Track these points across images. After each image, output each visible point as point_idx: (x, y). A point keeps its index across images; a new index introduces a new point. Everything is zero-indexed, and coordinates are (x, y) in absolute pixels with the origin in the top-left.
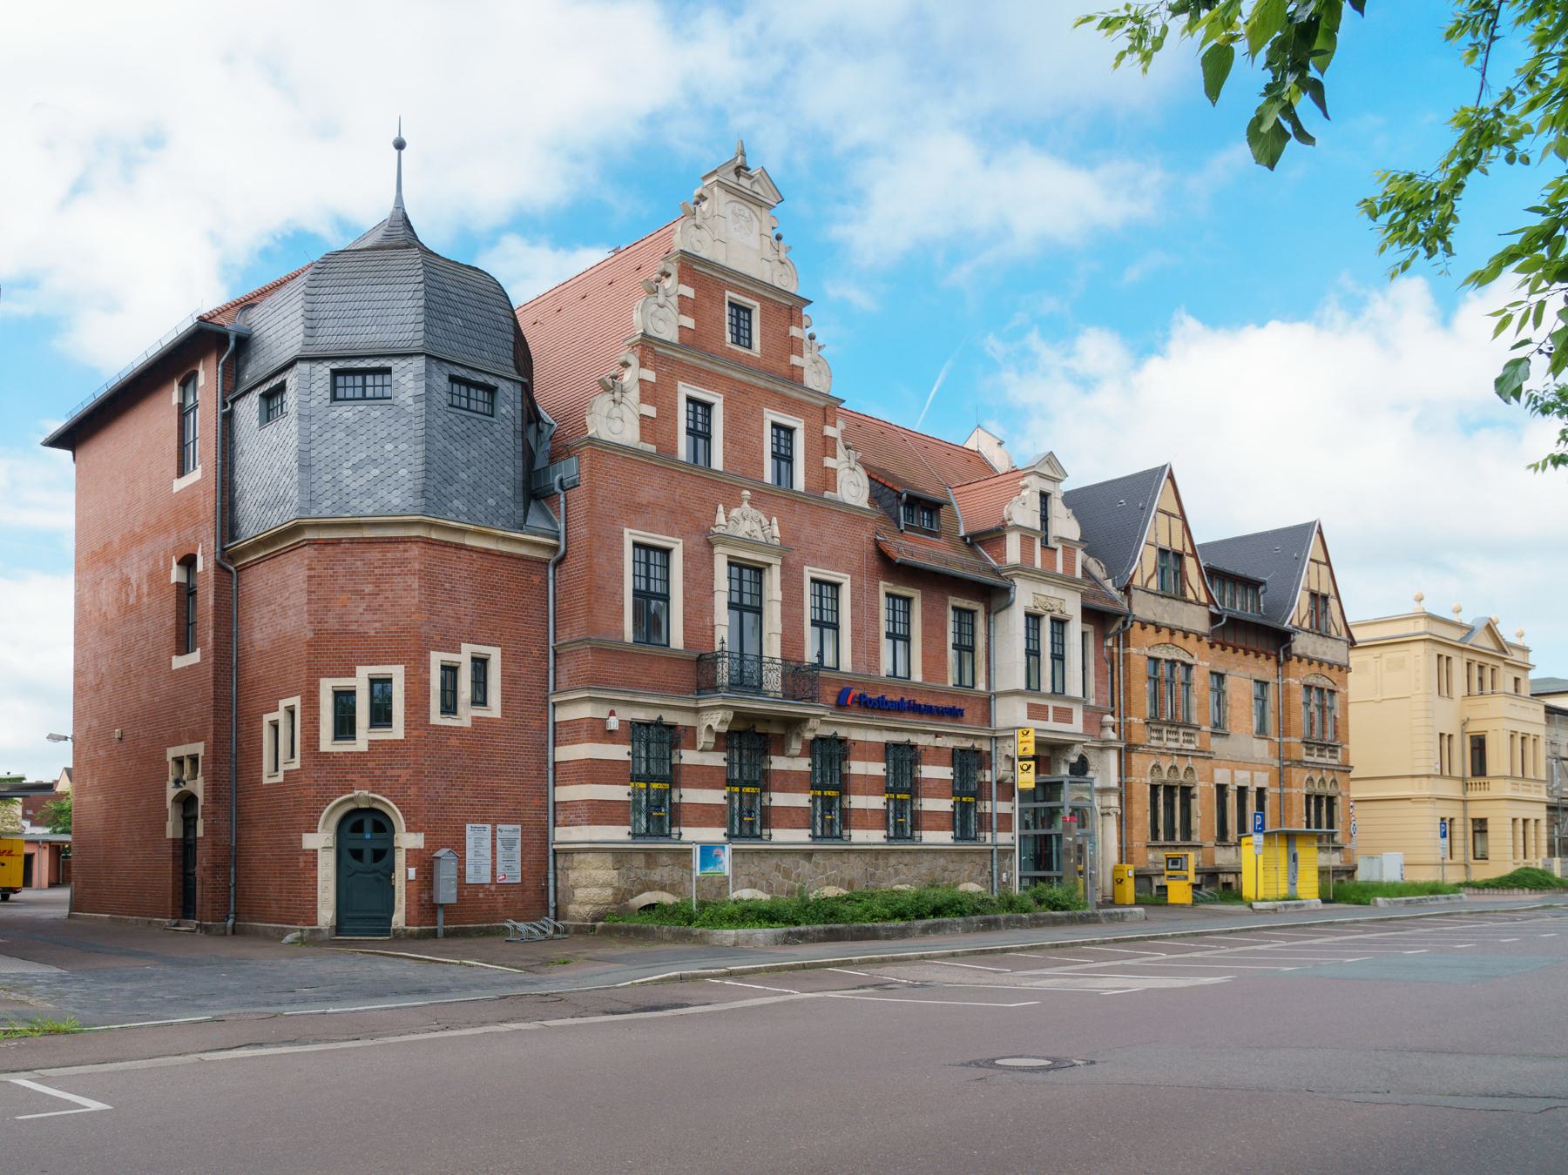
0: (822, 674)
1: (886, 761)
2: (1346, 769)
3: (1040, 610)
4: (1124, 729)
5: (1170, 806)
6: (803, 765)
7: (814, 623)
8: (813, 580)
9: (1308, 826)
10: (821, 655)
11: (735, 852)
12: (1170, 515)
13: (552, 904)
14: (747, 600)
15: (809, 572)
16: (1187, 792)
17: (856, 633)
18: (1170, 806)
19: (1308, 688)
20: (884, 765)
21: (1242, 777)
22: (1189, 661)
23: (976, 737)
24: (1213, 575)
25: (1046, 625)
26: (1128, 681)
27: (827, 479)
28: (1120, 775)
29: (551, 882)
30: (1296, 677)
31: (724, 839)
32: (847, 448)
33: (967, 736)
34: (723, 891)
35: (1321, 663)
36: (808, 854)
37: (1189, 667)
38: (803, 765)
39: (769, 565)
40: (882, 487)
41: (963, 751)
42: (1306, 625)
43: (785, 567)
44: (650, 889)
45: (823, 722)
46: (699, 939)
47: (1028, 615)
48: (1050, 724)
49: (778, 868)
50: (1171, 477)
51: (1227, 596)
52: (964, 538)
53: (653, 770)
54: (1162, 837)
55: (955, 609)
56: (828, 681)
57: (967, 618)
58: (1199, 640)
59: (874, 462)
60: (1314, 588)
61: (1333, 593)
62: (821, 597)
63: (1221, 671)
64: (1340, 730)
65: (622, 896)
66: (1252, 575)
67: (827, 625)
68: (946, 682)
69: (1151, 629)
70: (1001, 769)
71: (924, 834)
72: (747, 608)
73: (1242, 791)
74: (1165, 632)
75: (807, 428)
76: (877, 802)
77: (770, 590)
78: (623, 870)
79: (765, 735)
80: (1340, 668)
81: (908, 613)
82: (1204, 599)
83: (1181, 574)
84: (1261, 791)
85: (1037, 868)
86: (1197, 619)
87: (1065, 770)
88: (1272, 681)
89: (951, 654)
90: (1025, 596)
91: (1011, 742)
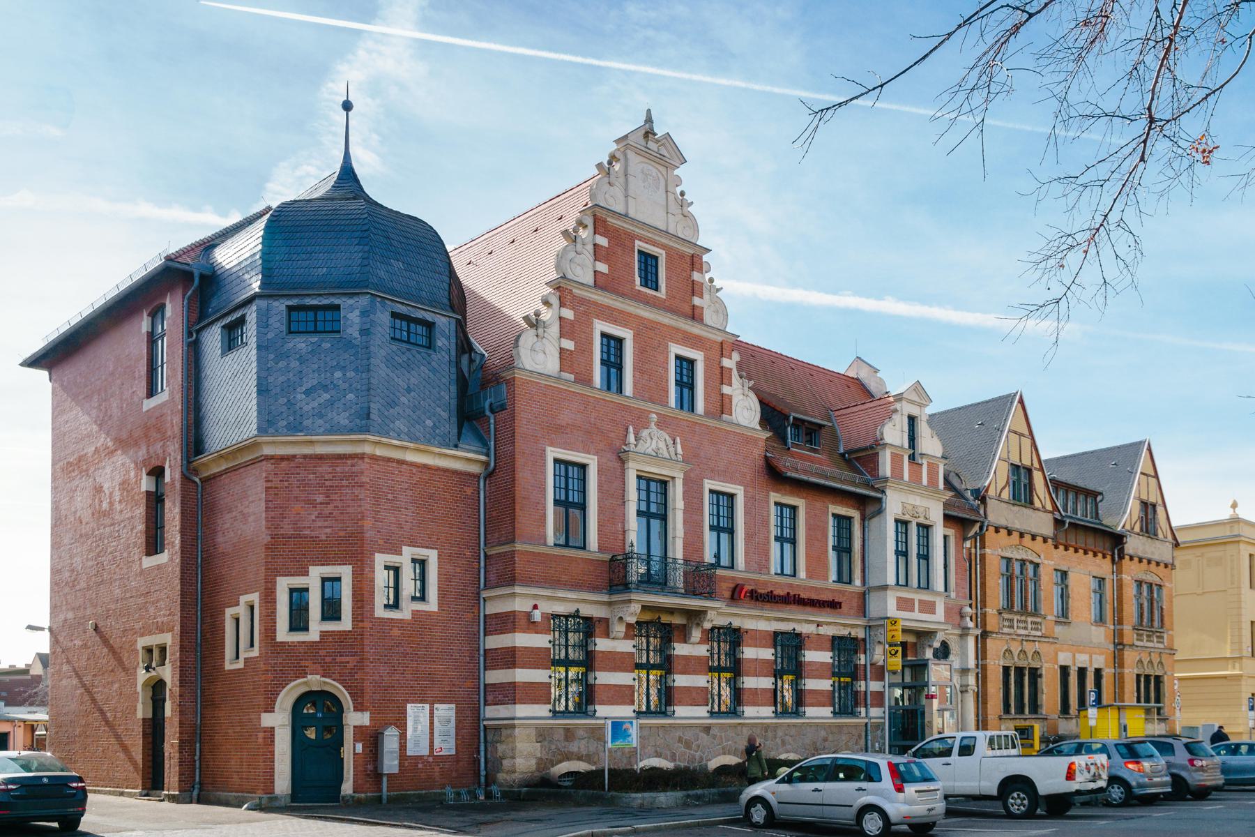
0: (719, 572)
1: (775, 647)
2: (1172, 651)
3: (907, 518)
4: (982, 620)
5: (1020, 684)
6: (702, 650)
7: (712, 528)
8: (712, 491)
9: (1139, 701)
10: (717, 556)
11: (641, 727)
12: (1021, 435)
13: (483, 773)
14: (653, 509)
15: (709, 484)
16: (1035, 674)
17: (749, 537)
18: (1020, 684)
19: (1140, 583)
20: (831, 654)
21: (1082, 660)
22: (1037, 560)
23: (853, 626)
24: (1057, 486)
25: (913, 529)
26: (983, 577)
27: (722, 406)
28: (977, 658)
29: (482, 753)
30: (1128, 574)
31: (634, 715)
32: (741, 377)
33: (845, 625)
34: (633, 760)
35: (1149, 562)
36: (707, 729)
37: (1037, 566)
38: (702, 650)
39: (673, 478)
40: (772, 416)
41: (841, 638)
42: (1137, 529)
43: (686, 481)
44: (568, 759)
45: (719, 614)
46: (611, 802)
47: (897, 521)
48: (916, 615)
49: (680, 740)
50: (1021, 402)
51: (1070, 504)
52: (843, 455)
53: (571, 656)
54: (1013, 711)
55: (834, 515)
56: (724, 578)
57: (844, 523)
58: (1045, 541)
59: (766, 388)
60: (1144, 497)
61: (1160, 502)
62: (718, 505)
63: (1065, 569)
64: (1166, 619)
65: (544, 764)
66: (1091, 486)
67: (724, 528)
68: (826, 579)
69: (1003, 532)
70: (878, 655)
71: (807, 709)
72: (656, 513)
73: (1082, 672)
74: (1016, 535)
75: (707, 359)
76: (825, 685)
77: (674, 500)
78: (546, 743)
79: (670, 625)
80: (1166, 566)
81: (794, 519)
82: (1049, 507)
83: (1030, 487)
84: (1098, 672)
85: (905, 739)
86: (1043, 524)
87: (929, 654)
88: (1109, 577)
89: (832, 556)
90: (895, 503)
91: (881, 630)
